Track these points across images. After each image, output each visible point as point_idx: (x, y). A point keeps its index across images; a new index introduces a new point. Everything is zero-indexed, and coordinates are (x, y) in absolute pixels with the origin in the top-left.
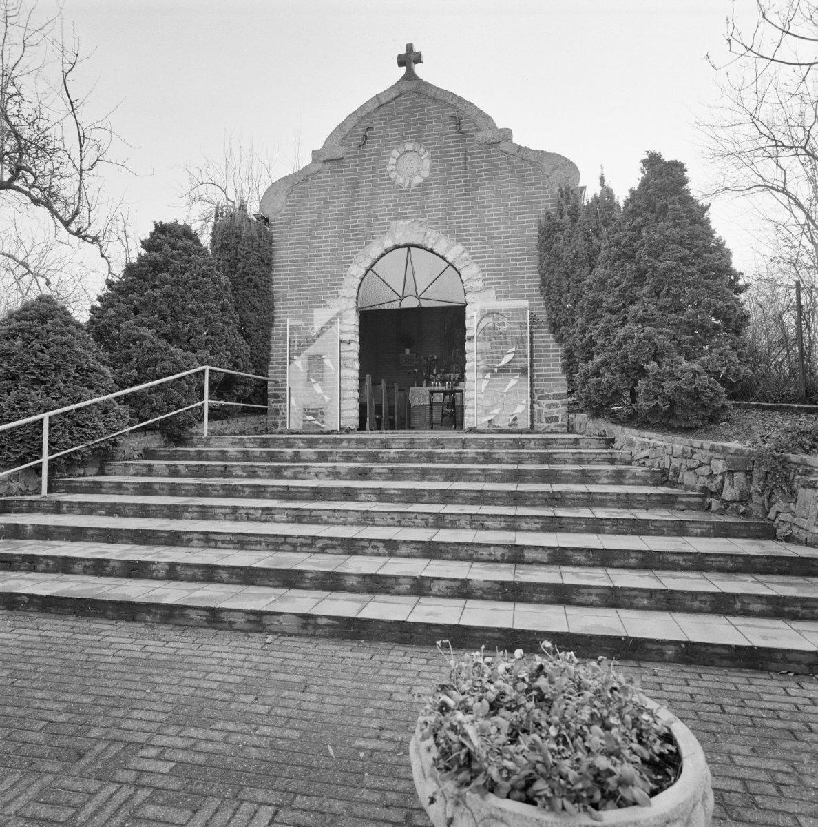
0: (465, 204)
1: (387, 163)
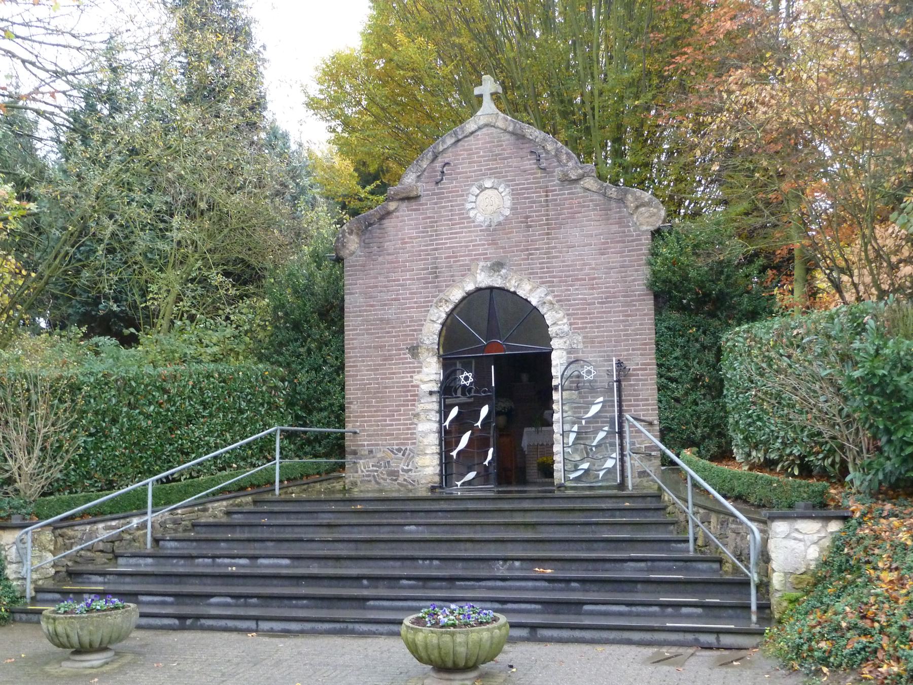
0: (548, 244)
1: (465, 200)
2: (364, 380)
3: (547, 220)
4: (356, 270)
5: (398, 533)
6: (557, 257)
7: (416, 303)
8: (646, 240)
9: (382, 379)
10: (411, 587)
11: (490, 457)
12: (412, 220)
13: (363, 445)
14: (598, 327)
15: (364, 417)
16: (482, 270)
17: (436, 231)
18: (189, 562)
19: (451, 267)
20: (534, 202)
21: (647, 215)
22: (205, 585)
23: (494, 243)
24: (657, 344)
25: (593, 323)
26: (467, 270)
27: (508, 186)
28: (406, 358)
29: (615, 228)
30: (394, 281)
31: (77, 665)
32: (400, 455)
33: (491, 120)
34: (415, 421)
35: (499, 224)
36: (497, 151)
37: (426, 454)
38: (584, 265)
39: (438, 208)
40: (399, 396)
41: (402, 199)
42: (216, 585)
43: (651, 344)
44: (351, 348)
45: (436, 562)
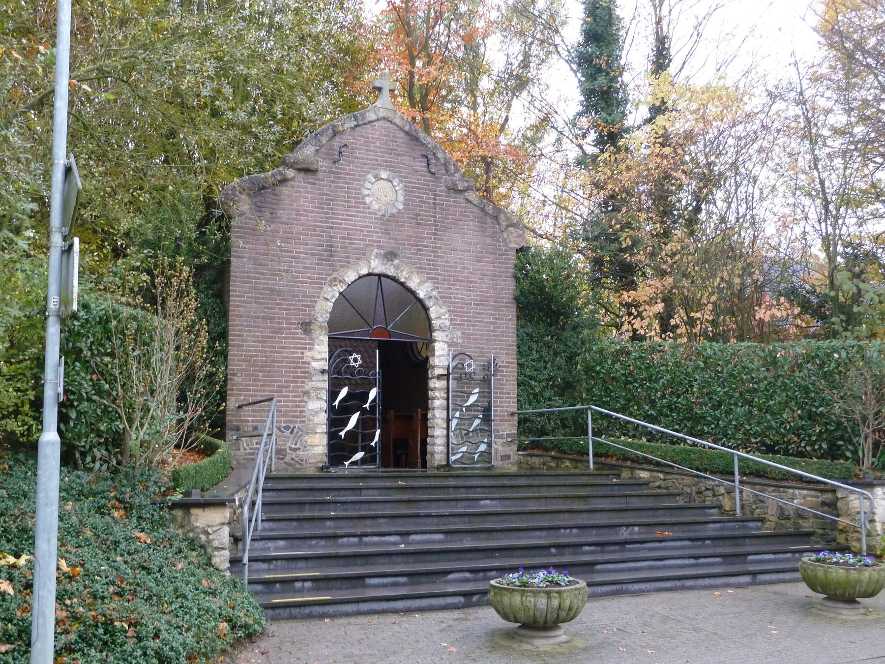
0: (435, 243)
1: (362, 186)
2: (250, 351)
3: (435, 221)
4: (246, 233)
5: (473, 507)
6: (442, 257)
7: (309, 278)
8: (512, 255)
9: (270, 352)
10: (591, 553)
11: (376, 439)
12: (308, 193)
13: (248, 421)
14: (473, 326)
15: (250, 390)
16: (376, 257)
17: (332, 209)
18: (331, 542)
19: (346, 248)
20: (424, 202)
21: (515, 234)
22: (394, 563)
23: (387, 232)
24: (518, 347)
25: (470, 321)
26: (362, 255)
27: (402, 182)
28: (297, 334)
29: (489, 241)
30: (287, 251)
31: (551, 641)
32: (288, 433)
33: (389, 114)
34: (306, 398)
35: (393, 215)
36: (392, 145)
37: (316, 433)
38: (464, 268)
39: (335, 187)
40: (289, 372)
41: (300, 170)
42: (408, 563)
43: (513, 345)
44: (237, 316)
45: (575, 531)
